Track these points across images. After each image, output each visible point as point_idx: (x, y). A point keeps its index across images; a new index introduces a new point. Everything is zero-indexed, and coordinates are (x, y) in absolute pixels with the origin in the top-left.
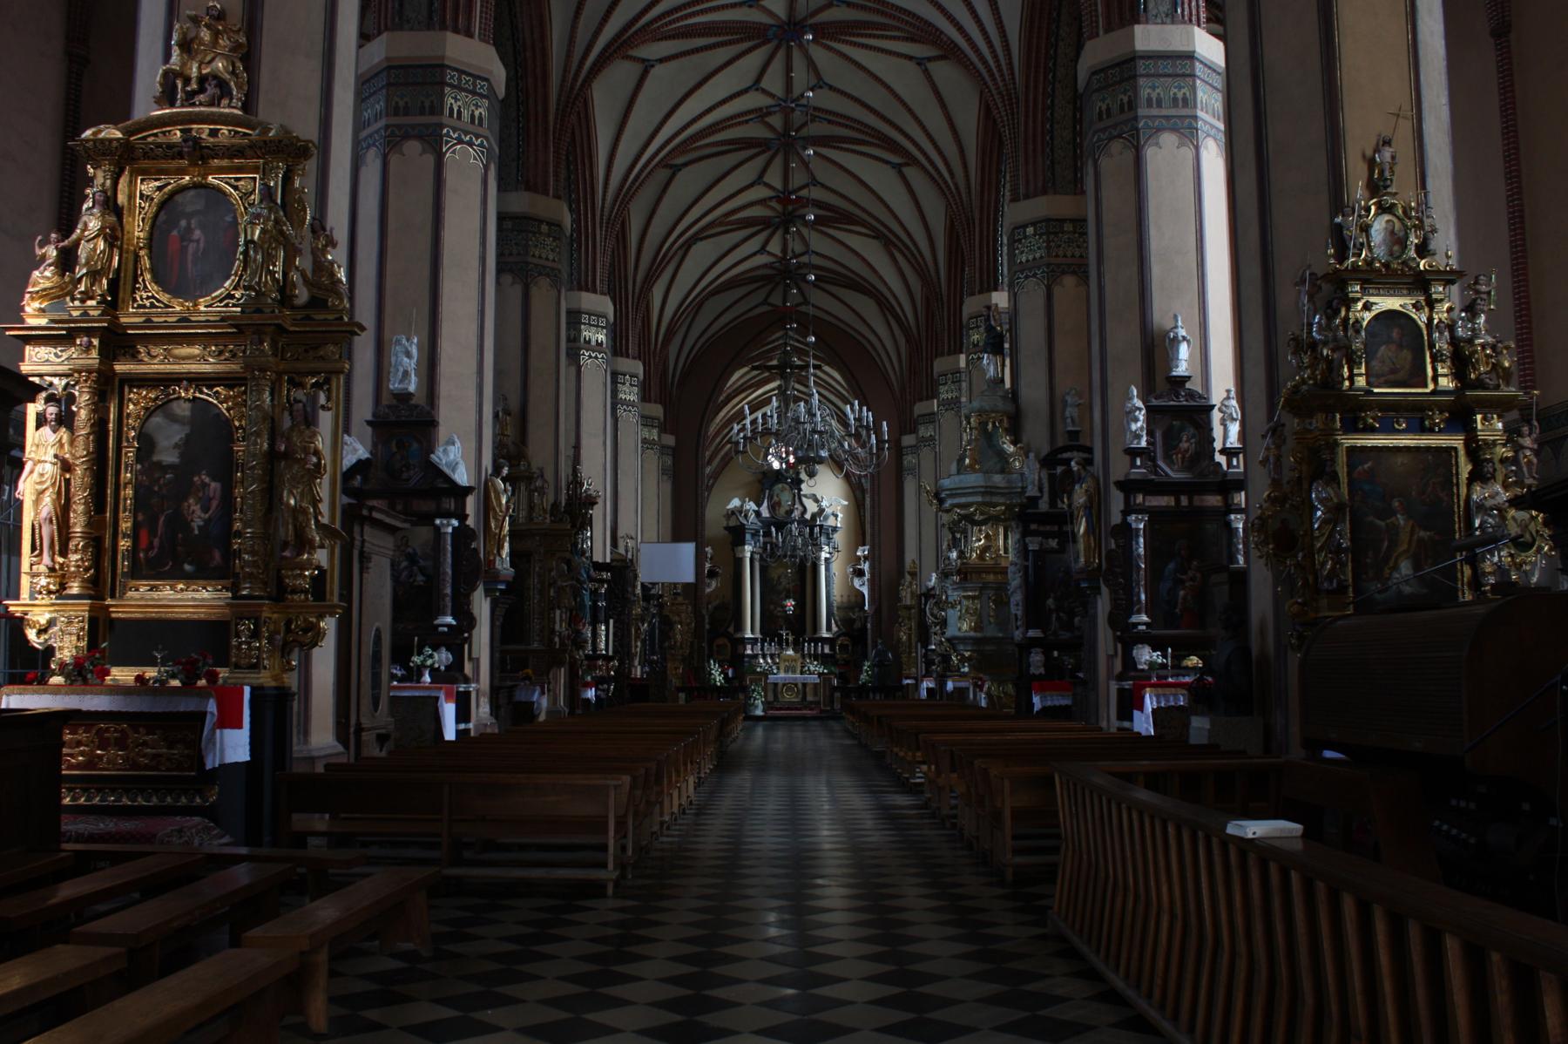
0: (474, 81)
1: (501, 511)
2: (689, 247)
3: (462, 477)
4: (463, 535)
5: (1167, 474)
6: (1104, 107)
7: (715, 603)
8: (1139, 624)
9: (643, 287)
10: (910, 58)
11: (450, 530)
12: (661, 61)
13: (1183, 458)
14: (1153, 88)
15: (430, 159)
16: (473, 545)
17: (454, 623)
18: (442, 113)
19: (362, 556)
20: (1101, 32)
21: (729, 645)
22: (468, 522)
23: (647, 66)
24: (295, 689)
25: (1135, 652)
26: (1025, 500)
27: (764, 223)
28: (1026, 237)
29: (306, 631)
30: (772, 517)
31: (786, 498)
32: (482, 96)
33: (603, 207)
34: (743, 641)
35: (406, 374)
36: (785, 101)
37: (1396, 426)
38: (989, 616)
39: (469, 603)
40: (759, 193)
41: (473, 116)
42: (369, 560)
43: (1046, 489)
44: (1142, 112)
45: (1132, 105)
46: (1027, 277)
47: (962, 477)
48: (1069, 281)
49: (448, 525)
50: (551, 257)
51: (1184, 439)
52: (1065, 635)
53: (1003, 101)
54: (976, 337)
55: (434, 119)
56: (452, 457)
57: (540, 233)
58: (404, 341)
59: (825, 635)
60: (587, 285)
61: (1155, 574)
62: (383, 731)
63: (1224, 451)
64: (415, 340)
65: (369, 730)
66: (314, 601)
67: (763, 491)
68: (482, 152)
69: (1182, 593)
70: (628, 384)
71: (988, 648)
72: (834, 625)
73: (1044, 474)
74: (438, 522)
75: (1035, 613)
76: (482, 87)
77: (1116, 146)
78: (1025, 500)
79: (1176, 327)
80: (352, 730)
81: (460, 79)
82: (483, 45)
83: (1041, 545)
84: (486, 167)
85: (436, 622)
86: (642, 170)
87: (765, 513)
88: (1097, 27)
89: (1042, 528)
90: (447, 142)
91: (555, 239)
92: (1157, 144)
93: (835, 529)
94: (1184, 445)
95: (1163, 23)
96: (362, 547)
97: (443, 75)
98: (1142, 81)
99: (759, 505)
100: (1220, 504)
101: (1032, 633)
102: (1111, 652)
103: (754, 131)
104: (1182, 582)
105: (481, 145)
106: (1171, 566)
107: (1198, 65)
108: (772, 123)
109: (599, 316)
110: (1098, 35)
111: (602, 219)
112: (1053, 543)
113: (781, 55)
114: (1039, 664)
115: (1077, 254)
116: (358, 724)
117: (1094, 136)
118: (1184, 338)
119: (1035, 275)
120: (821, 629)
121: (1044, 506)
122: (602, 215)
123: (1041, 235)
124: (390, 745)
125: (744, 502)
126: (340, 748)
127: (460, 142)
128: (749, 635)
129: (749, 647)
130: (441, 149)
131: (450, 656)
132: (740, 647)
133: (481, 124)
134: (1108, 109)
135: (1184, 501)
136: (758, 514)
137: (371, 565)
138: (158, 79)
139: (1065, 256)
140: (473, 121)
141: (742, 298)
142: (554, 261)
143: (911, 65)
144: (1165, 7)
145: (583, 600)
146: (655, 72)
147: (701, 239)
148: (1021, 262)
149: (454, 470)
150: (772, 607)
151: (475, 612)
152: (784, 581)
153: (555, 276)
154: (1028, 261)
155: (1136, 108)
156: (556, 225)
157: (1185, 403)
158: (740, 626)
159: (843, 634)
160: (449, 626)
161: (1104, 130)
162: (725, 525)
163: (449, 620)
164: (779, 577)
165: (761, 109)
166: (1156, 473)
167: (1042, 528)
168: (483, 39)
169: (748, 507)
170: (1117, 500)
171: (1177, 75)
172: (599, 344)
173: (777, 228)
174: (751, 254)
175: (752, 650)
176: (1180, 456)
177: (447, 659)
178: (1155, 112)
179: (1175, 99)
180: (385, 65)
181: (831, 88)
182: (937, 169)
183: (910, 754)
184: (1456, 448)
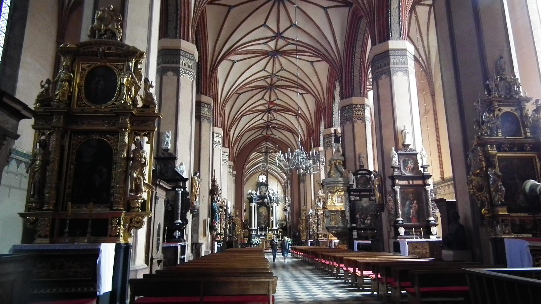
0: (190, 55)
1: (196, 187)
2: (242, 118)
3: (185, 175)
4: (185, 194)
5: (405, 174)
6: (379, 65)
8: (400, 221)
9: (229, 128)
10: (309, 61)
11: (180, 192)
12: (238, 61)
13: (409, 169)
14: (395, 59)
15: (175, 78)
16: (188, 197)
17: (181, 222)
18: (179, 64)
19: (156, 197)
20: (377, 43)
22: (186, 190)
23: (234, 62)
24: (132, 244)
25: (399, 230)
26: (349, 185)
27: (263, 111)
28: (346, 109)
29: (138, 222)
32: (192, 60)
33: (220, 103)
34: (252, 230)
35: (167, 143)
36: (272, 74)
37: (514, 149)
38: (339, 220)
39: (186, 216)
40: (262, 102)
41: (189, 65)
42: (158, 199)
43: (355, 182)
44: (391, 66)
45: (388, 64)
46: (347, 121)
47: (330, 179)
48: (359, 122)
49: (180, 190)
50: (208, 114)
51: (409, 163)
52: (362, 226)
53: (339, 71)
54: (327, 140)
55: (177, 65)
56: (182, 169)
57: (205, 107)
58: (167, 133)
60: (215, 125)
61: (403, 206)
62: (160, 259)
63: (422, 167)
64: (170, 133)
65: (155, 259)
66: (141, 211)
67: (258, 188)
68: (192, 77)
69: (412, 211)
70: (225, 155)
71: (339, 230)
73: (354, 177)
74: (177, 189)
75: (353, 220)
76: (192, 57)
77: (384, 76)
78: (349, 185)
79: (405, 129)
80: (150, 259)
81: (185, 54)
82: (192, 44)
83: (354, 198)
84: (193, 81)
85: (175, 222)
86: (231, 93)
87: (258, 194)
88: (376, 42)
89: (355, 194)
90: (181, 73)
91: (209, 109)
92: (396, 75)
94: (409, 165)
95: (397, 40)
96: (156, 194)
97: (180, 52)
98: (391, 57)
99: (256, 192)
100: (422, 183)
101: (354, 225)
102: (389, 230)
103: (262, 83)
104: (412, 207)
105: (191, 74)
106: (408, 203)
107: (408, 52)
108: (267, 81)
109: (219, 134)
110: (376, 45)
111: (220, 106)
112: (358, 198)
113: (272, 60)
114: (356, 235)
115: (361, 114)
116: (152, 257)
117: (376, 74)
118: (408, 133)
119: (349, 120)
121: (354, 187)
122: (220, 105)
123: (351, 109)
124: (162, 264)
126: (146, 266)
127: (185, 73)
128: (253, 228)
129: (254, 232)
130: (179, 74)
131: (180, 233)
132: (251, 232)
133: (191, 68)
134: (381, 66)
135: (411, 182)
136: (256, 194)
137: (158, 201)
138: (89, 29)
139: (358, 115)
140: (189, 67)
141: (255, 132)
142: (209, 115)
143: (309, 63)
144: (398, 35)
145: (216, 216)
146: (235, 64)
147: (245, 115)
148: (345, 117)
149: (182, 173)
150: (260, 220)
151: (188, 218)
152: (263, 213)
153: (209, 119)
154: (347, 116)
155: (390, 65)
156: (209, 105)
157: (409, 152)
158: (251, 226)
160: (180, 223)
161: (379, 72)
163: (180, 221)
164: (262, 212)
165: (265, 76)
166: (401, 174)
167: (355, 194)
168: (192, 42)
170: (389, 182)
171: (402, 55)
172: (219, 142)
173: (266, 113)
174: (259, 120)
176: (408, 168)
177: (179, 234)
178: (395, 66)
179: (401, 62)
180: (162, 49)
181: (285, 70)
182: (315, 94)
183: (331, 263)
184: (535, 157)
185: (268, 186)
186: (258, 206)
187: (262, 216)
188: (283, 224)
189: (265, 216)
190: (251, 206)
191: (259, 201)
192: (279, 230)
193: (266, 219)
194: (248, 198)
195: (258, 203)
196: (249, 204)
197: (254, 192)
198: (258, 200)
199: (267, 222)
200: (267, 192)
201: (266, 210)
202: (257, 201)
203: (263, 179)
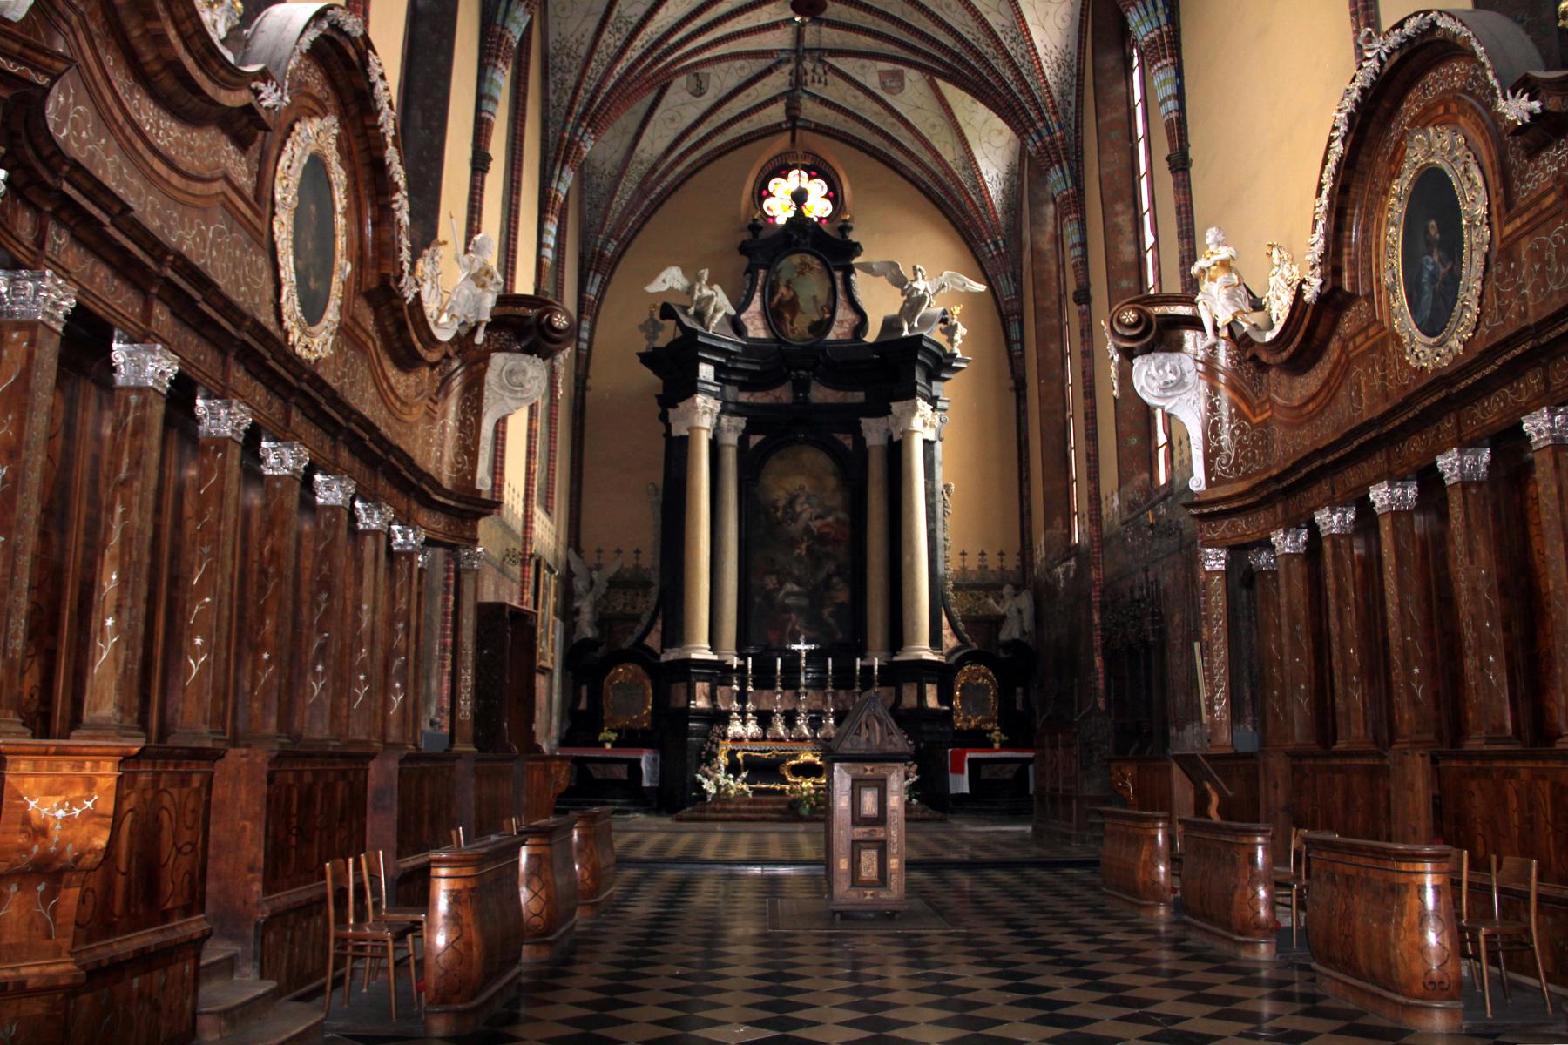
7: (612, 569)
21: (648, 683)
30: (778, 340)
31: (811, 289)
34: (687, 670)
59: (928, 655)
72: (946, 631)
87: (756, 328)
93: (941, 365)
120: (914, 639)
125: (694, 278)
128: (701, 651)
129: (702, 687)
132: (680, 689)
136: (736, 325)
152: (805, 511)
158: (677, 632)
159: (973, 657)
162: (643, 347)
164: (791, 502)
169: (706, 292)
175: (712, 697)
185: (856, 261)
186: (755, 440)
187: (793, 543)
188: (999, 621)
189: (821, 538)
190: (679, 430)
191: (760, 398)
192: (961, 679)
193: (830, 567)
194: (650, 359)
195: (756, 419)
196: (664, 418)
197: (721, 304)
198: (751, 383)
199: (842, 595)
200: (844, 314)
201: (831, 482)
202: (744, 397)
203: (799, 197)
